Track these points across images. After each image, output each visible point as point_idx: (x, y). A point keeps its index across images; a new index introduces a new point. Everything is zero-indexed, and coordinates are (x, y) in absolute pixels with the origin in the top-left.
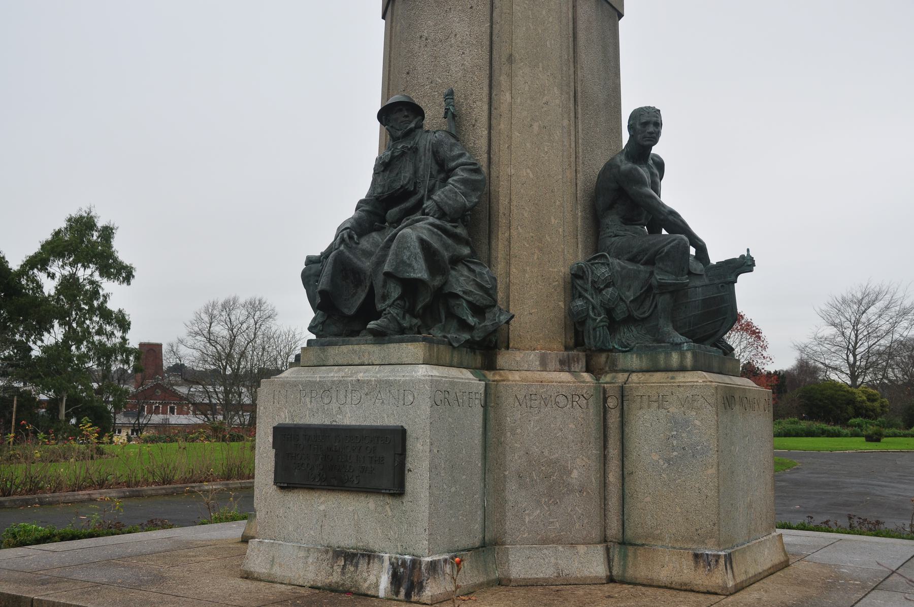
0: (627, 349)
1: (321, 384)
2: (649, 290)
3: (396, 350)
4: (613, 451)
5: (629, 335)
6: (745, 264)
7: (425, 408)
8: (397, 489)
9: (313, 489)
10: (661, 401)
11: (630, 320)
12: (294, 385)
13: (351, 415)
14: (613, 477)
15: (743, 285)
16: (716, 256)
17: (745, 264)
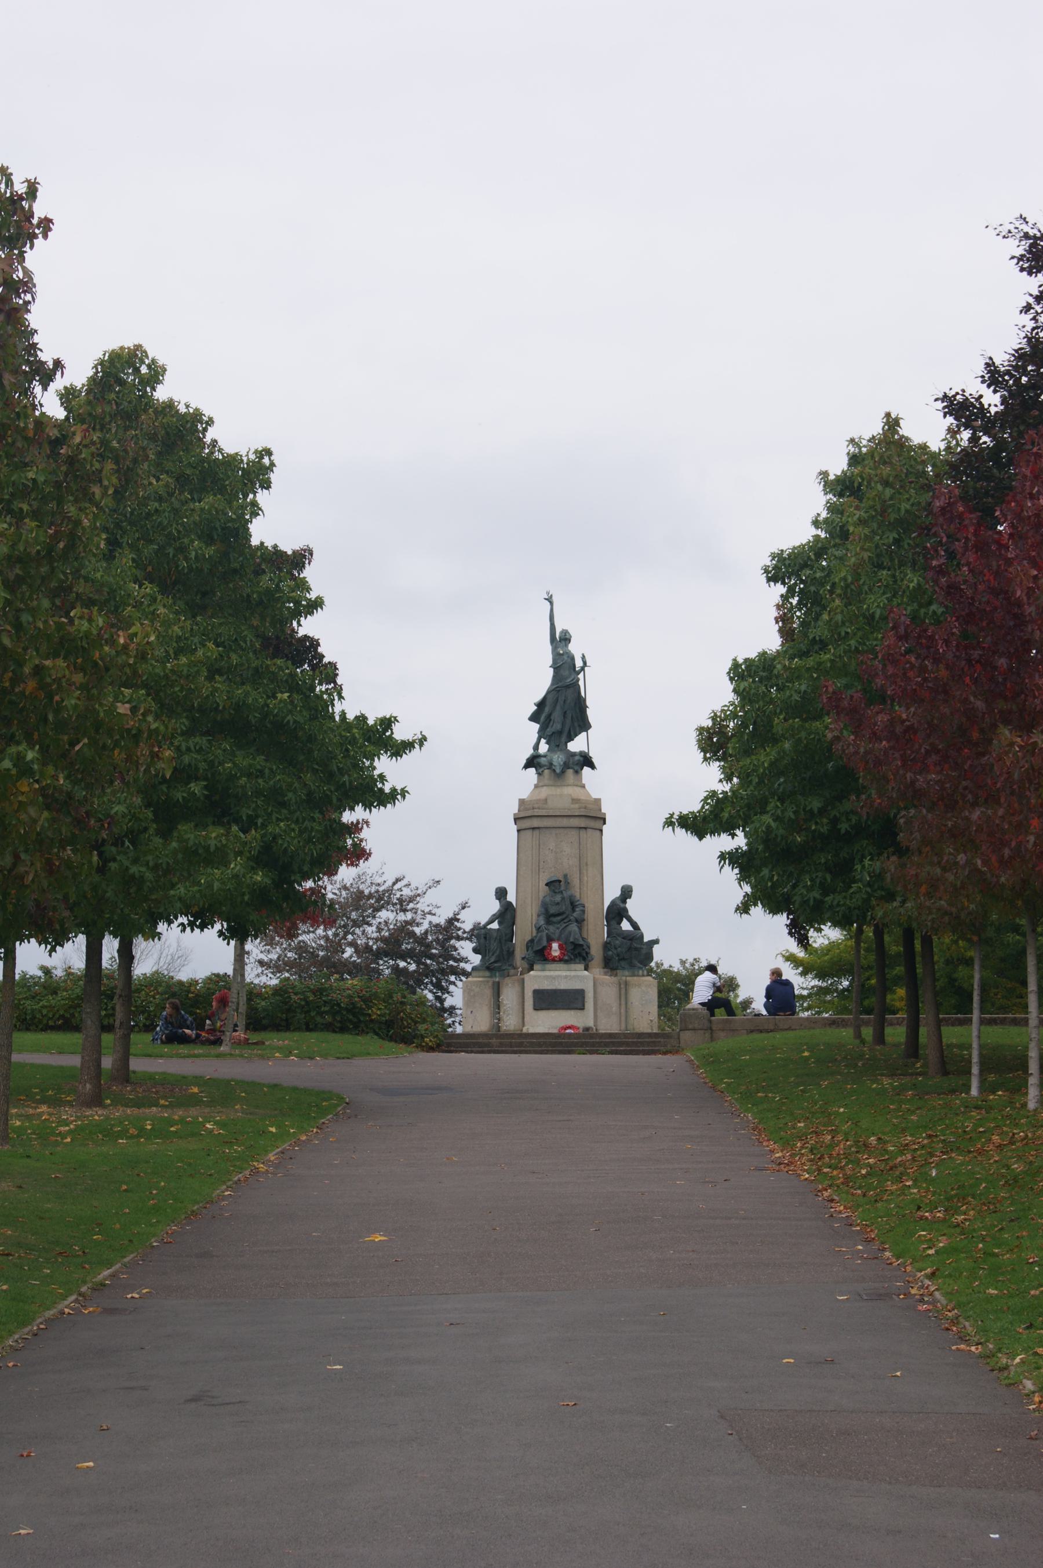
0: (624, 968)
1: (551, 976)
2: (630, 949)
3: (573, 966)
4: (623, 1002)
5: (623, 963)
6: (656, 942)
7: (592, 984)
8: (582, 1008)
9: (548, 1009)
10: (639, 986)
11: (624, 959)
12: (535, 976)
13: (563, 986)
14: (623, 1011)
15: (656, 949)
16: (646, 940)
17: (657, 942)
